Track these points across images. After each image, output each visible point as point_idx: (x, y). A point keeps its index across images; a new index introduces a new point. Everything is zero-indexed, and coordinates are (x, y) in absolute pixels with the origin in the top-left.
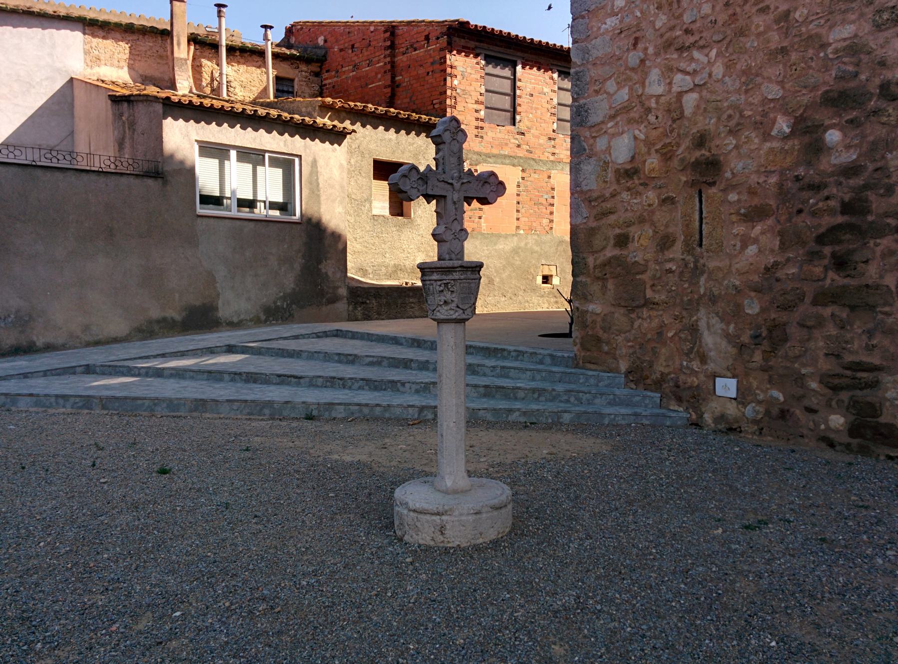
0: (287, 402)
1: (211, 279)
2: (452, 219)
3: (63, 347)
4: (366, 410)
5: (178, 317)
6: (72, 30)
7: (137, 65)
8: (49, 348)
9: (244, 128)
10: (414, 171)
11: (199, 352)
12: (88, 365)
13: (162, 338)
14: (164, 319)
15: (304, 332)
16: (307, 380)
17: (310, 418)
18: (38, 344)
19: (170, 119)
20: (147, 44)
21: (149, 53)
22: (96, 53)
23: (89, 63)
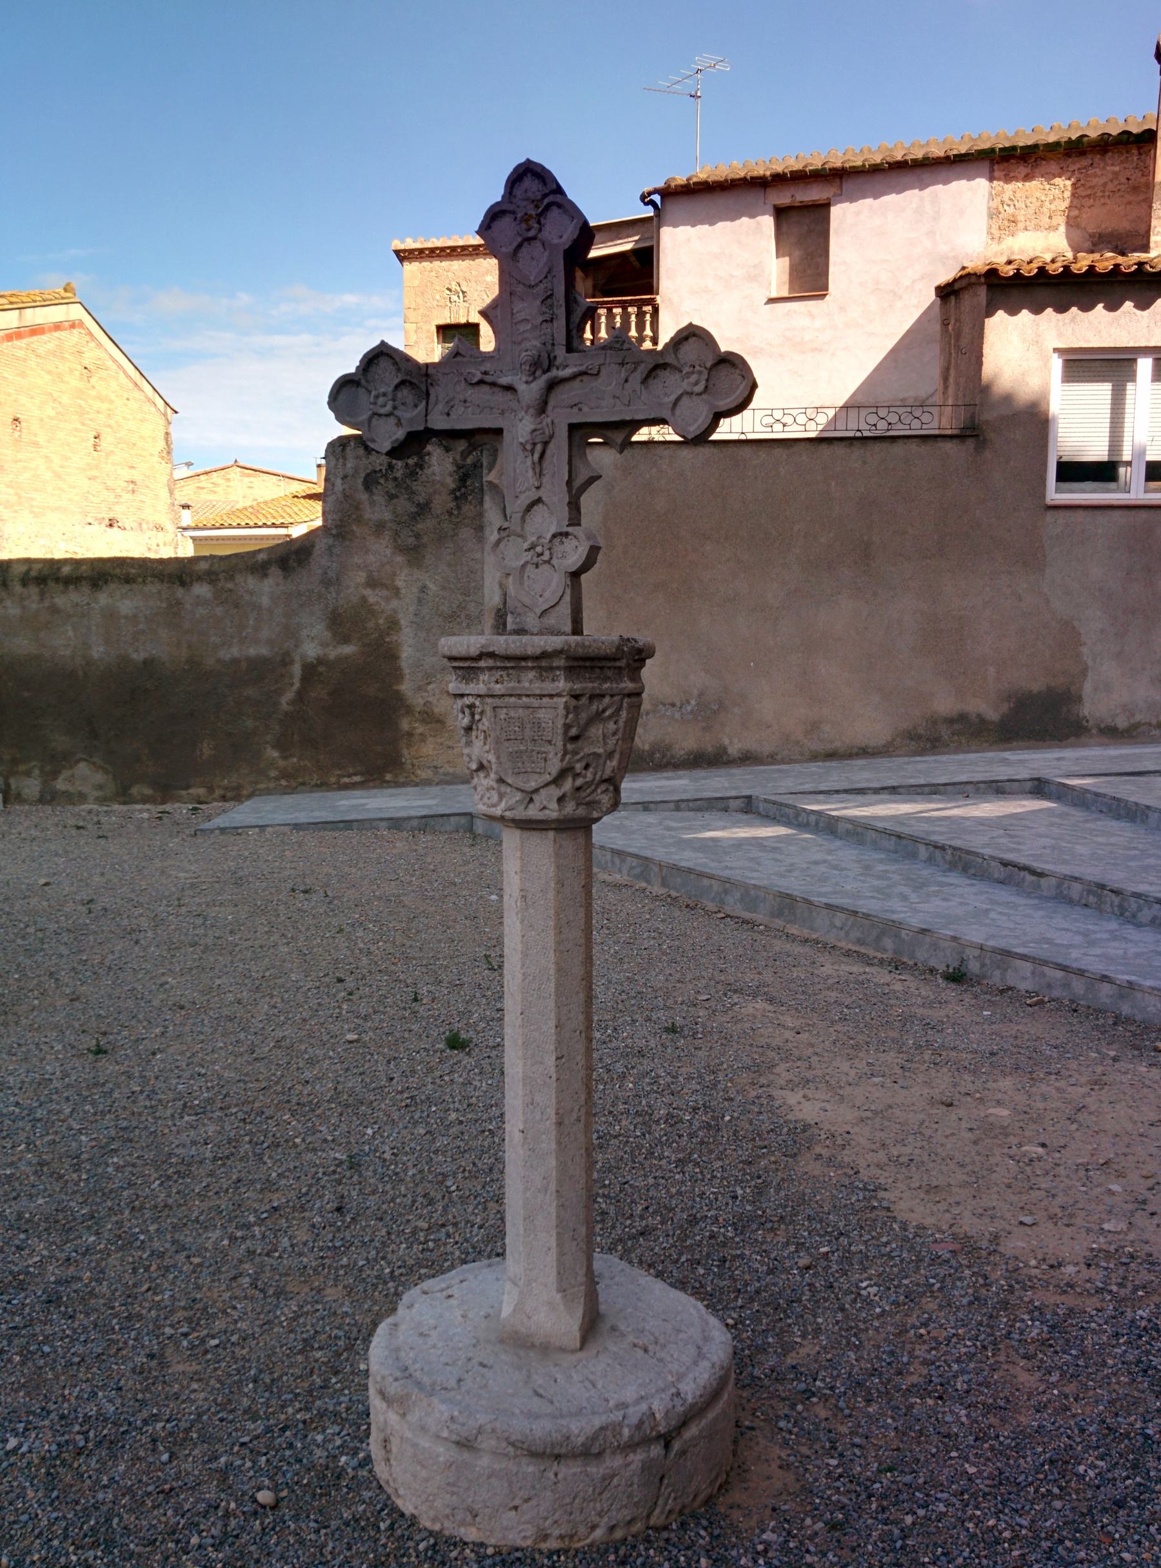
0: (924, 931)
1: (1069, 636)
2: (524, 500)
3: (772, 759)
4: (1078, 986)
5: (993, 715)
6: (970, 179)
7: (1086, 214)
8: (747, 759)
9: (1112, 307)
10: (384, 363)
11: (969, 787)
12: (749, 797)
13: (956, 752)
14: (962, 717)
15: (1002, 773)
16: (1053, 881)
17: (957, 977)
18: (730, 751)
19: (1001, 314)
20: (1111, 168)
21: (1110, 186)
22: (1010, 210)
23: (996, 233)
